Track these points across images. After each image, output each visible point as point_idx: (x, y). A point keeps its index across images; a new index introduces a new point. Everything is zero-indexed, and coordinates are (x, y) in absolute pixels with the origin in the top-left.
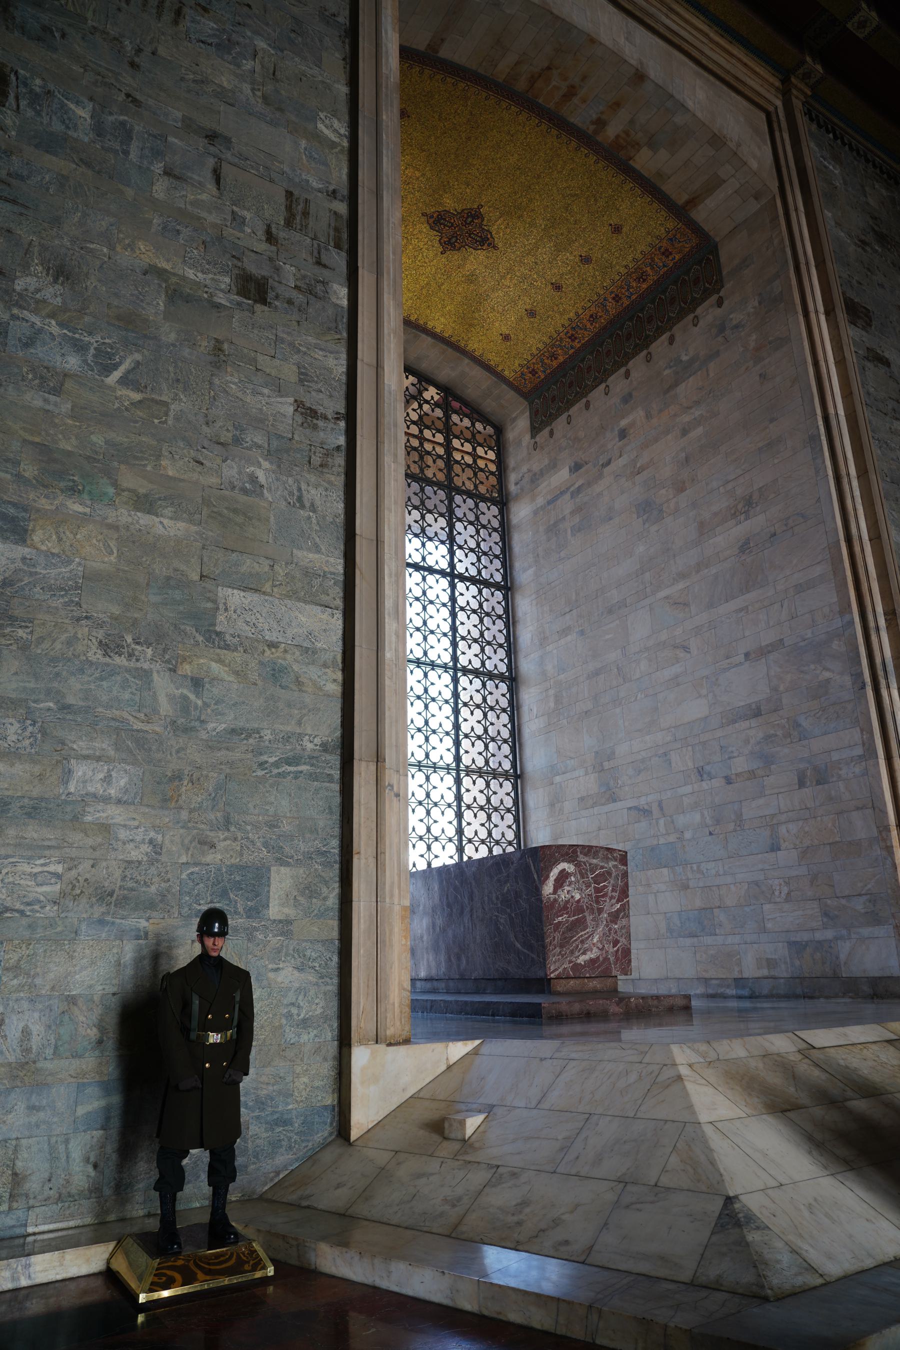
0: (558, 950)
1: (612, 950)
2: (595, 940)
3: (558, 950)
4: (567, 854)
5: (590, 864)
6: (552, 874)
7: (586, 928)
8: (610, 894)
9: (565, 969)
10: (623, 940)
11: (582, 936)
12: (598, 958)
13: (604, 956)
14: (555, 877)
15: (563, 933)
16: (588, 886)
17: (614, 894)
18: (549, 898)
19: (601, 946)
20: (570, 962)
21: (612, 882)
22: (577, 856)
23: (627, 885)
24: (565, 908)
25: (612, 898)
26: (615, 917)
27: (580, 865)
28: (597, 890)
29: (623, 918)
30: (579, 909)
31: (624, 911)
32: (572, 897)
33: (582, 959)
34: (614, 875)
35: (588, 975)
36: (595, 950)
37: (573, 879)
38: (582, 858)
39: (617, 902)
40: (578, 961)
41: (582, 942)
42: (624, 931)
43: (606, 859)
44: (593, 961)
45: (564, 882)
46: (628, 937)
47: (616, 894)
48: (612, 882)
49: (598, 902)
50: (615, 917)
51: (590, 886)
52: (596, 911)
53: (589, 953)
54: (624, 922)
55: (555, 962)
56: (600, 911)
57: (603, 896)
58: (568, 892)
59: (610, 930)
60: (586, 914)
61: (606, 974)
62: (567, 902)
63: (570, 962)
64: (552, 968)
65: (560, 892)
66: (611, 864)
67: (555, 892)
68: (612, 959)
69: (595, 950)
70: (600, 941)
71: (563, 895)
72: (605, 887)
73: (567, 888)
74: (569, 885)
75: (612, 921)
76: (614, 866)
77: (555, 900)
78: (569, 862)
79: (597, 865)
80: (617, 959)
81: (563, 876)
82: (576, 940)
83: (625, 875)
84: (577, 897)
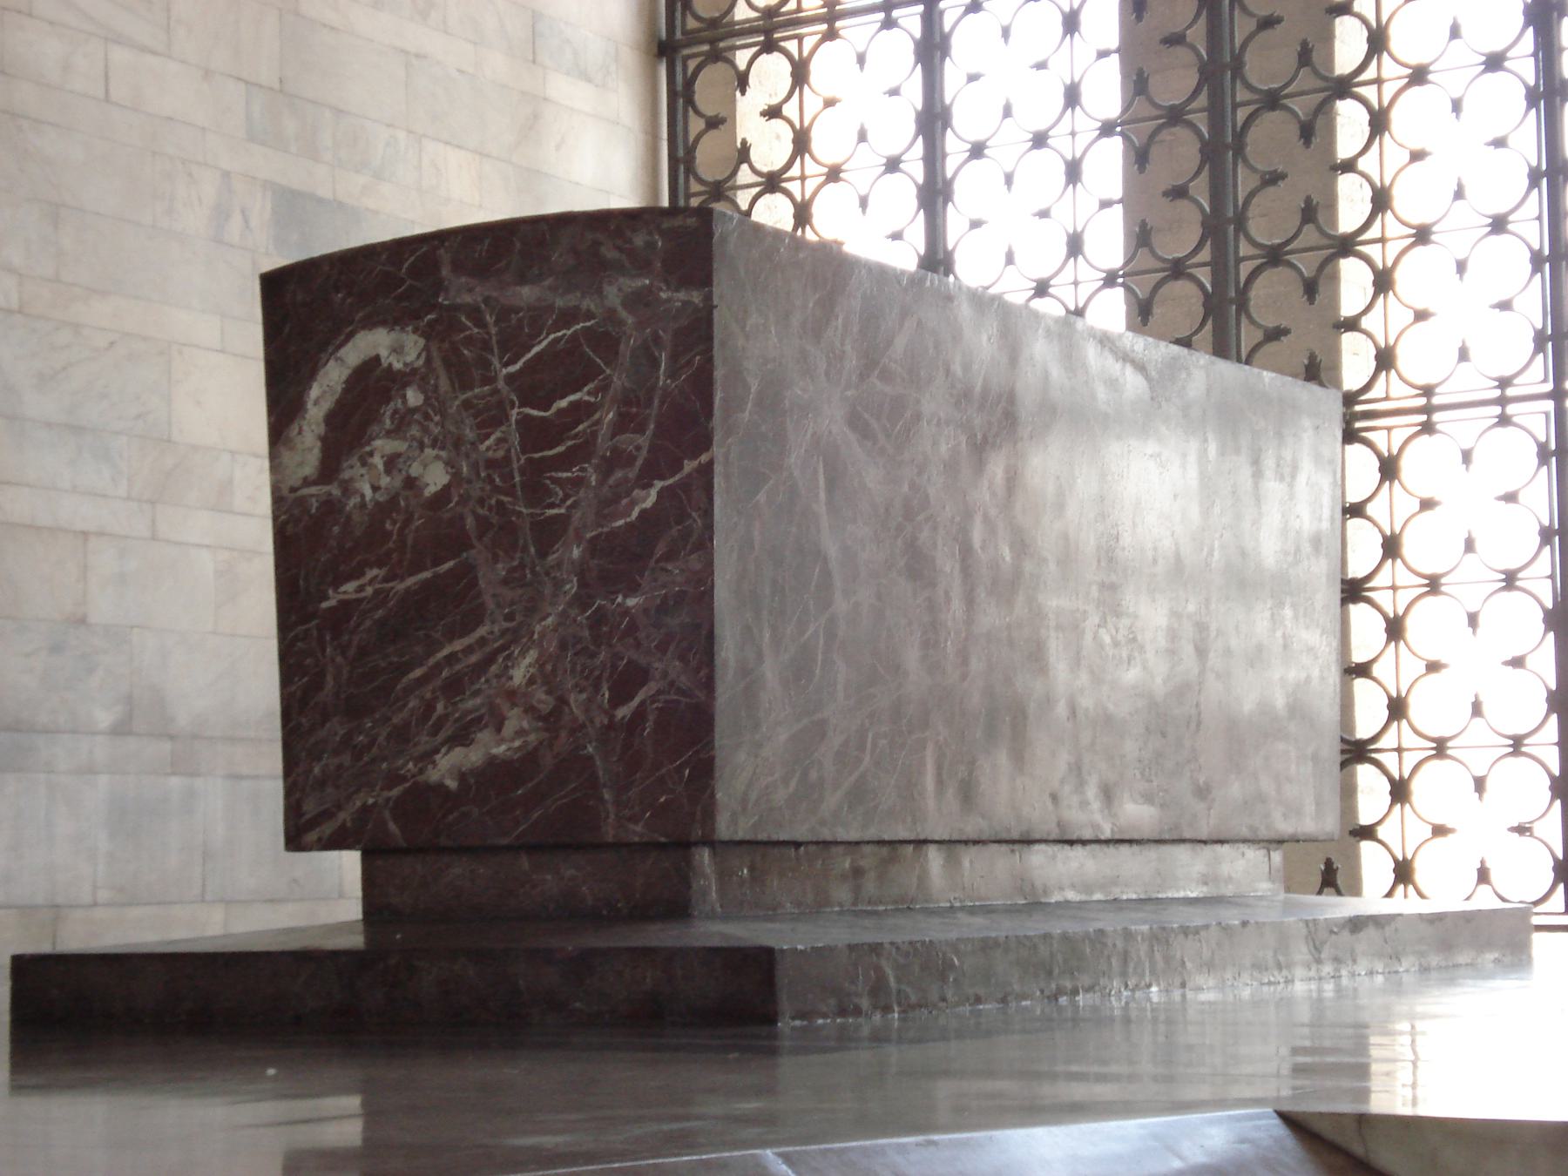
0: (336, 728)
2: (519, 675)
3: (336, 728)
5: (504, 313)
6: (315, 392)
7: (475, 617)
8: (603, 445)
9: (365, 809)
10: (668, 668)
11: (451, 659)
12: (530, 758)
14: (327, 405)
16: (491, 418)
17: (628, 441)
20: (394, 779)
21: (619, 381)
22: (439, 287)
26: (622, 558)
29: (670, 556)
30: (441, 531)
32: (411, 483)
33: (447, 766)
36: (515, 720)
37: (414, 397)
38: (462, 292)
39: (644, 483)
40: (433, 776)
41: (454, 688)
42: (674, 622)
44: (497, 775)
45: (373, 417)
47: (640, 443)
48: (619, 381)
49: (536, 492)
50: (622, 558)
51: (500, 420)
53: (484, 736)
55: (321, 783)
56: (549, 533)
57: (565, 461)
58: (391, 463)
59: (598, 620)
60: (477, 554)
61: (570, 836)
63: (394, 779)
64: (310, 808)
65: (352, 469)
66: (613, 295)
67: (329, 469)
70: (545, 676)
71: (367, 482)
72: (580, 411)
73: (383, 446)
74: (396, 432)
76: (637, 301)
77: (330, 507)
78: (394, 321)
79: (538, 319)
81: (372, 385)
83: (697, 333)
84: (435, 478)
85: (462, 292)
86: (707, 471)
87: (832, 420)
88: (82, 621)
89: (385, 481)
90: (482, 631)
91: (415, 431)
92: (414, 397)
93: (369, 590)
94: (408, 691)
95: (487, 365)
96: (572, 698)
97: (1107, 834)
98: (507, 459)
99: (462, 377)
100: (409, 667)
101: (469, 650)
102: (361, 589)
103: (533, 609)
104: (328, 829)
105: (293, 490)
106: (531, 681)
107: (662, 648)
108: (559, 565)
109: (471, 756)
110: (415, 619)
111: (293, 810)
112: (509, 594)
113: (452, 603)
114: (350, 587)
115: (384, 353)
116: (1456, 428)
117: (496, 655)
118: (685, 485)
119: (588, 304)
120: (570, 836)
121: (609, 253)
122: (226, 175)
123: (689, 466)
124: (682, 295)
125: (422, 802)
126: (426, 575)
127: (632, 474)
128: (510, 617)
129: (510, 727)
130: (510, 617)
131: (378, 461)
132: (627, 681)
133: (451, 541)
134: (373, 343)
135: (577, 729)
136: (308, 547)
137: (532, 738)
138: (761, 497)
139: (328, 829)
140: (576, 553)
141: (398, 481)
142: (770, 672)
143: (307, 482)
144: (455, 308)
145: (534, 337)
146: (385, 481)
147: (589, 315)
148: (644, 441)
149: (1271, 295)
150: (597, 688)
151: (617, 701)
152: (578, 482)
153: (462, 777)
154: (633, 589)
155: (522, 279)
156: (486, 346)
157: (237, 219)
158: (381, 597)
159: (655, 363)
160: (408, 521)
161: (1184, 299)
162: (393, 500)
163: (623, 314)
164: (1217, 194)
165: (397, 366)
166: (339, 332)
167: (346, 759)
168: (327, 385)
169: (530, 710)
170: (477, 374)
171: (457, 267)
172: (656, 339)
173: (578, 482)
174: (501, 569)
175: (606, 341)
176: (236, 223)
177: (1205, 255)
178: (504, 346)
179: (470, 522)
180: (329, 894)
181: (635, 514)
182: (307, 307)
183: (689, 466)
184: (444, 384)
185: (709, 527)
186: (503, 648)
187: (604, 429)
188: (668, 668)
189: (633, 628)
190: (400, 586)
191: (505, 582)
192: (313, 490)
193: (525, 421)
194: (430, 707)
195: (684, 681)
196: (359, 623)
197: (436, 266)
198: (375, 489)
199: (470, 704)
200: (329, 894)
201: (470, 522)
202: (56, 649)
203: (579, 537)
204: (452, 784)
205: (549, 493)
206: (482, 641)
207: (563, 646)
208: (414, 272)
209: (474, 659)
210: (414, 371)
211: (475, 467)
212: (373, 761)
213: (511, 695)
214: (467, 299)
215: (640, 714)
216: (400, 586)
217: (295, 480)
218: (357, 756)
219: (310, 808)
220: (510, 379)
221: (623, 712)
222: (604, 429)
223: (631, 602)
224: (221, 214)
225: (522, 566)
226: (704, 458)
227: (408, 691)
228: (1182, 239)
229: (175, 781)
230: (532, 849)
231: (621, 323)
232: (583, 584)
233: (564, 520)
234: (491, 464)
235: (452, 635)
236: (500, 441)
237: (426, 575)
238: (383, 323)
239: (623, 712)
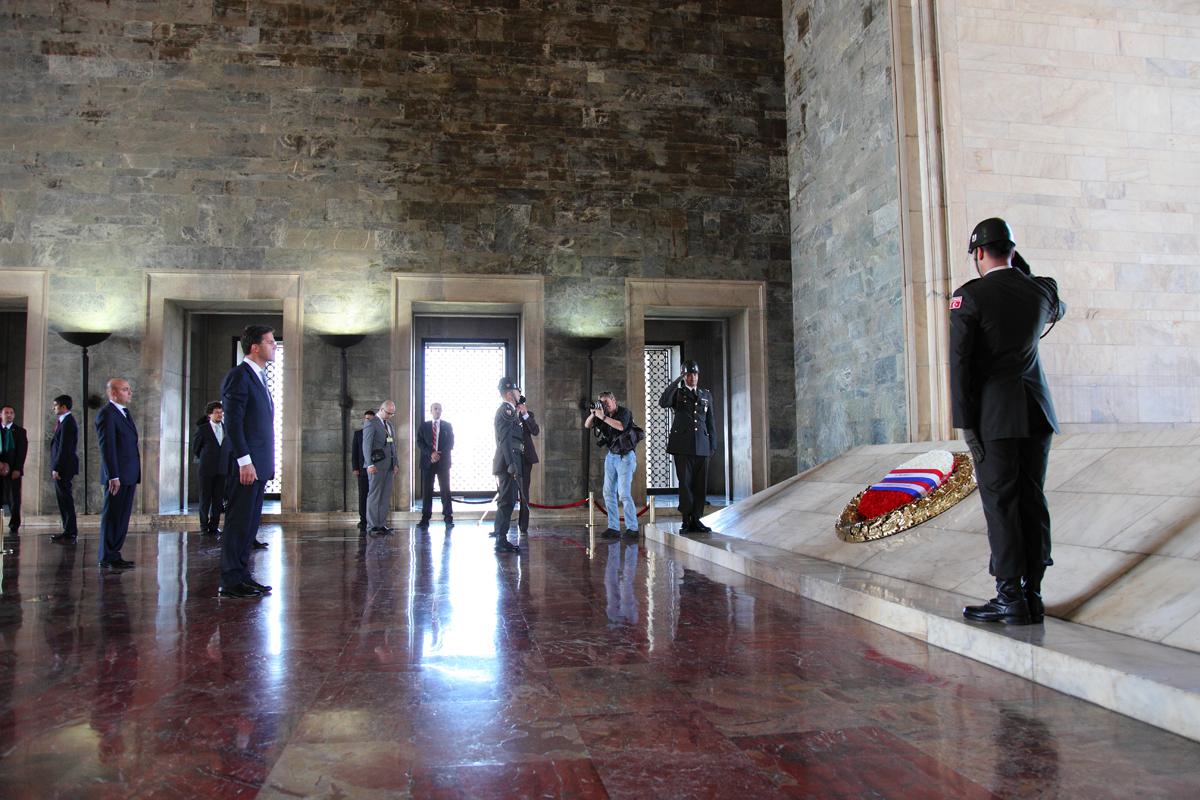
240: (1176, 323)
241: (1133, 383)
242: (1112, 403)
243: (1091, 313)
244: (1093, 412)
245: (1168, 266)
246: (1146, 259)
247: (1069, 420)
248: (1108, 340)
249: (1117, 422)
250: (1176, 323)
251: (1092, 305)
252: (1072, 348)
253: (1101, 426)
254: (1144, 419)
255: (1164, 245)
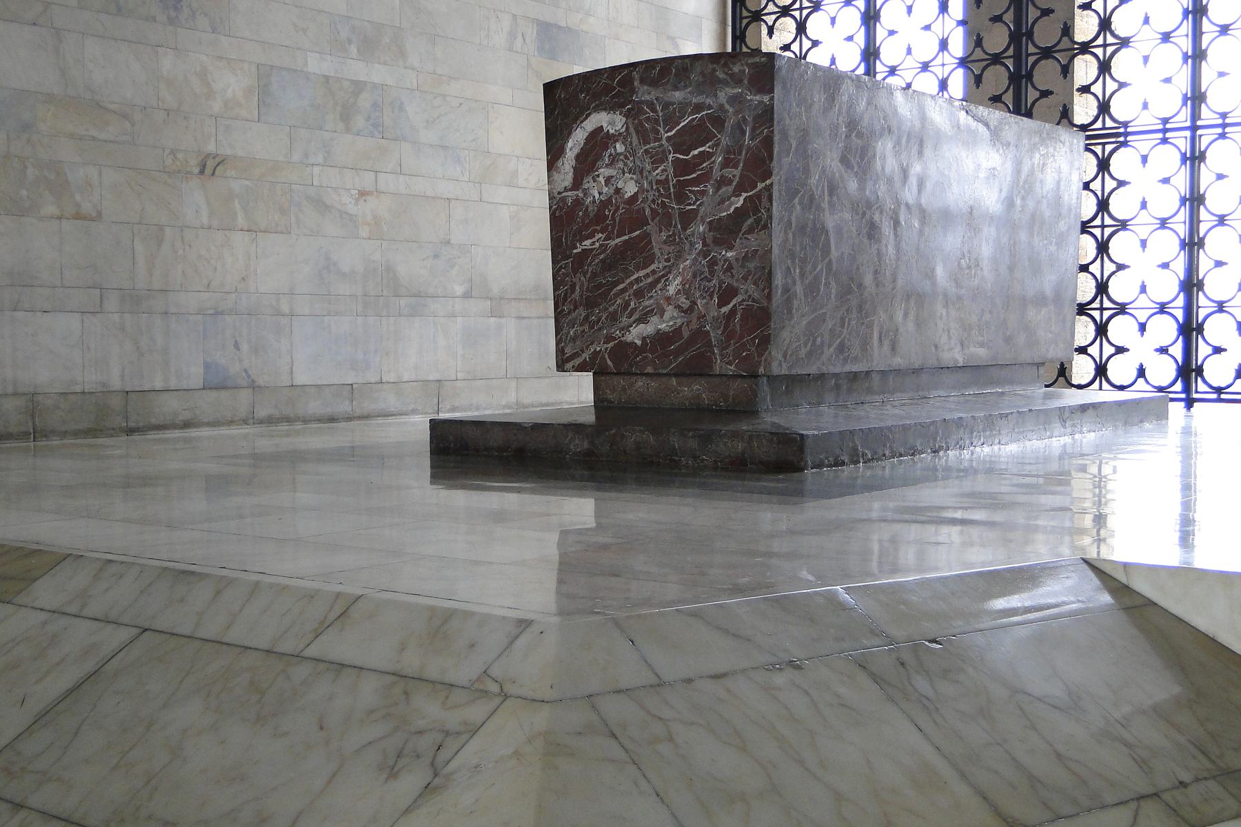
0: (582, 312)
1: (711, 309)
2: (672, 290)
3: (582, 312)
4: (608, 89)
5: (666, 106)
6: (570, 144)
7: (651, 259)
8: (716, 174)
11: (638, 280)
12: (677, 331)
13: (694, 326)
14: (576, 151)
15: (594, 275)
16: (658, 159)
18: (563, 199)
19: (685, 303)
20: (609, 338)
23: (768, 143)
24: (599, 218)
25: (723, 181)
26: (726, 231)
27: (641, 111)
28: (682, 168)
29: (751, 230)
31: (755, 215)
32: (618, 191)
33: (636, 334)
34: (729, 125)
35: (649, 370)
36: (670, 311)
37: (620, 147)
38: (644, 94)
40: (629, 338)
41: (639, 294)
42: (751, 265)
43: (710, 84)
44: (661, 340)
45: (599, 157)
46: (766, 277)
47: (735, 173)
48: (725, 141)
49: (681, 197)
50: (726, 231)
51: (663, 160)
52: (676, 219)
53: (655, 319)
54: (754, 241)
55: (574, 339)
56: (688, 218)
58: (608, 180)
59: (713, 263)
60: (651, 228)
62: (605, 204)
63: (609, 338)
64: (569, 351)
65: (588, 183)
66: (723, 96)
67: (577, 184)
68: (715, 335)
69: (670, 311)
70: (685, 291)
71: (596, 190)
72: (704, 156)
73: (604, 172)
74: (611, 165)
75: (717, 242)
76: (734, 100)
77: (578, 202)
78: (611, 108)
79: (683, 108)
80: (729, 335)
81: (599, 141)
82: (624, 290)
83: (766, 115)
84: (630, 189)
85: (644, 94)
86: (769, 188)
87: (831, 161)
88: (449, 242)
89: (605, 190)
90: (653, 267)
91: (621, 165)
92: (620, 147)
93: (597, 245)
94: (617, 295)
95: (657, 132)
96: (699, 302)
97: (961, 364)
98: (667, 180)
99: (644, 138)
100: (616, 284)
101: (647, 276)
102: (593, 243)
103: (679, 256)
104: (577, 362)
105: (559, 193)
106: (679, 292)
107: (745, 278)
108: (693, 234)
109: (648, 329)
110: (619, 260)
111: (560, 351)
112: (667, 248)
113: (639, 252)
114: (588, 242)
115: (605, 125)
116: (1142, 145)
117: (661, 279)
118: (758, 196)
119: (709, 101)
120: (698, 368)
121: (720, 74)
122: (514, 16)
123: (760, 186)
124: (758, 98)
125: (623, 351)
126: (626, 237)
127: (731, 189)
128: (668, 260)
129: (667, 316)
130: (668, 260)
131: (601, 179)
132: (727, 295)
133: (636, 220)
134: (600, 119)
135: (701, 317)
136: (565, 221)
137: (679, 322)
138: (796, 201)
139: (577, 362)
140: (701, 228)
141: (612, 191)
142: (799, 289)
143: (566, 190)
144: (641, 102)
145: (682, 117)
146: (605, 190)
147: (710, 107)
148: (737, 172)
149: (1045, 74)
150: (711, 297)
151: (720, 306)
152: (703, 193)
153: (644, 339)
154: (731, 248)
155: (676, 88)
156: (656, 121)
157: (520, 38)
158: (603, 248)
159: (744, 133)
160: (617, 209)
161: (997, 78)
162: (609, 200)
163: (727, 107)
164: (1018, 20)
165: (611, 131)
166: (582, 113)
167: (586, 327)
168: (576, 140)
169: (678, 307)
170: (652, 136)
171: (642, 81)
172: (744, 119)
173: (703, 193)
174: (664, 235)
175: (718, 120)
176: (519, 42)
177: (1011, 52)
178: (666, 123)
179: (648, 212)
180: (577, 393)
181: (732, 210)
182: (565, 101)
183: (760, 186)
184: (635, 140)
185: (770, 217)
186: (663, 276)
187: (716, 166)
188: (748, 290)
189: (730, 268)
190: (612, 243)
191: (665, 242)
192: (569, 193)
193: (676, 160)
194: (627, 304)
195: (756, 296)
196: (591, 259)
197: (631, 81)
198: (600, 194)
199: (647, 303)
200: (577, 393)
201: (648, 212)
202: (436, 256)
203: (703, 222)
204: (639, 342)
205: (688, 198)
206: (654, 272)
207: (694, 276)
208: (620, 84)
209: (650, 280)
210: (620, 134)
211: (651, 183)
212: (600, 329)
213: (668, 299)
214: (647, 97)
215: (733, 312)
216: (612, 243)
217: (560, 188)
218: (591, 327)
219: (569, 351)
220: (669, 139)
221: (725, 309)
222: (716, 166)
223: (729, 254)
224: (512, 35)
225: (674, 234)
226: (768, 182)
227: (617, 295)
228: (998, 40)
229: (492, 320)
230: (676, 375)
231: (727, 111)
232: (705, 244)
233: (696, 211)
234: (658, 182)
235: (638, 269)
236: (663, 171)
237: (626, 237)
238: (605, 110)
239: (725, 309)
240: (363, 194)
241: (285, 308)
242: (245, 347)
243: (210, 164)
244: (207, 366)
245: (353, 82)
246: (316, 64)
247: (158, 385)
248: (241, 221)
249: (253, 386)
250: (363, 194)
251: (211, 148)
252: (168, 232)
253: (224, 394)
254: (301, 379)
255: (350, 42)
